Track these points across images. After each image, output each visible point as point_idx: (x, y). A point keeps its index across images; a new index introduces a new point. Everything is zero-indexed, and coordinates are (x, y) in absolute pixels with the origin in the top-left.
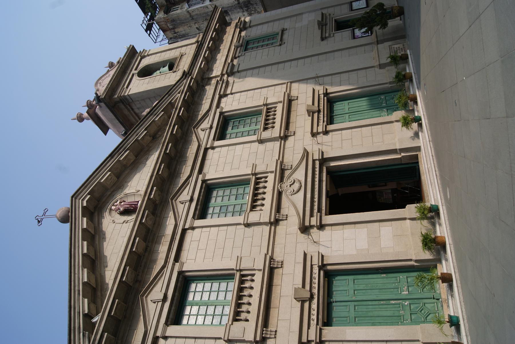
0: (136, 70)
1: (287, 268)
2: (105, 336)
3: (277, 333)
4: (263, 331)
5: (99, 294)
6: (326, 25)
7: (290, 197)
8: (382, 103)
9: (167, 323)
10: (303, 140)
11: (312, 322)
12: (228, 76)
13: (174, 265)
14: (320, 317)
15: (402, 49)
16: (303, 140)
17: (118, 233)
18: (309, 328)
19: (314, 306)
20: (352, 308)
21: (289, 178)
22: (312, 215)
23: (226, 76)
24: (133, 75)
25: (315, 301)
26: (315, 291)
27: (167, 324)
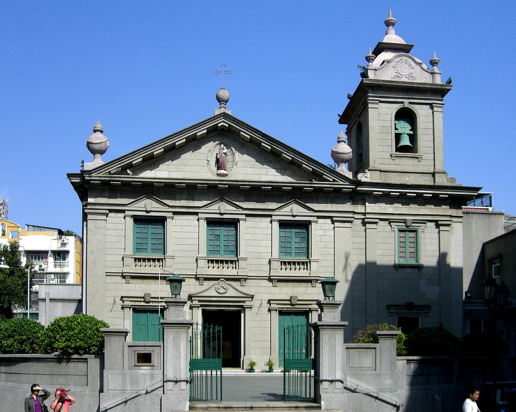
0: (410, 103)
7: (214, 287)
10: (263, 292)
12: (363, 219)
13: (171, 212)
18: (130, 301)
19: (143, 304)
20: (144, 323)
22: (199, 301)
23: (362, 217)
24: (403, 103)
26: (151, 304)
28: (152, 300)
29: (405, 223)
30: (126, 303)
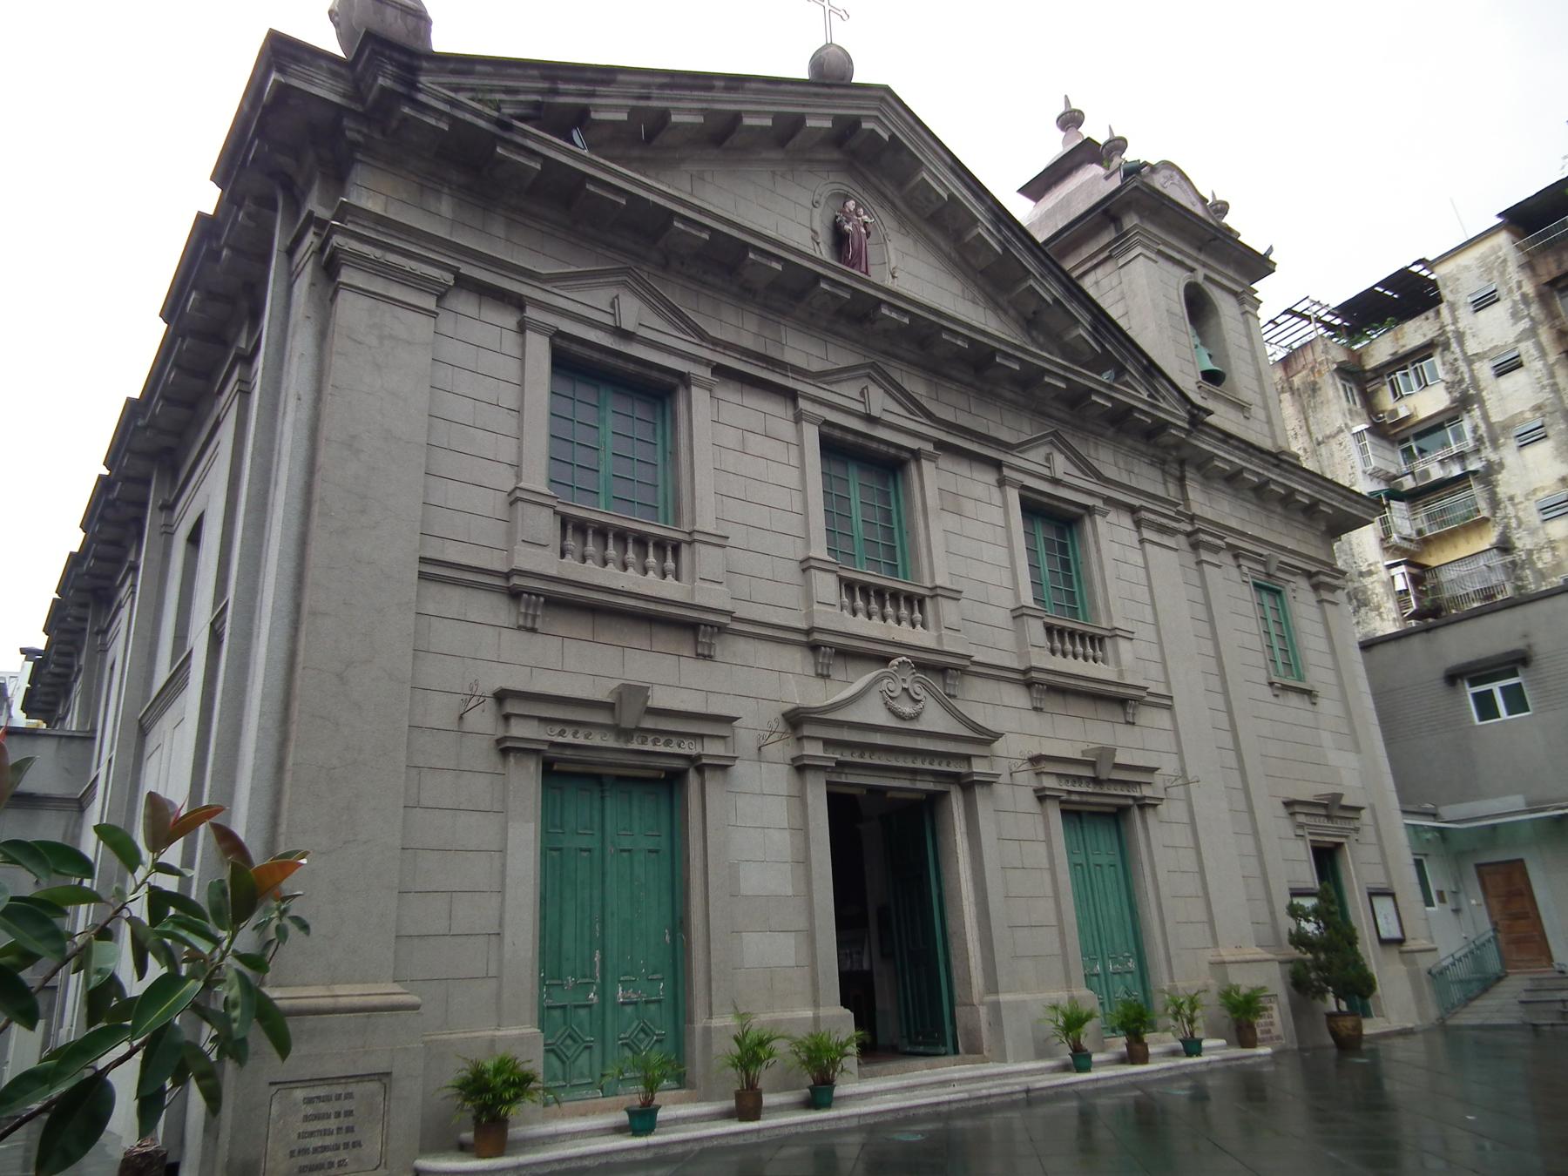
0: (1207, 278)
1: (694, 671)
2: (532, 164)
3: (527, 636)
4: (538, 595)
5: (635, 153)
6: (1328, 817)
7: (877, 689)
8: (1115, 960)
9: (559, 341)
10: (1022, 731)
11: (557, 729)
12: (1188, 535)
13: (708, 363)
14: (568, 753)
15: (1269, 1031)
16: (1022, 731)
17: (786, 214)
18: (541, 719)
19: (597, 740)
20: (584, 842)
21: (925, 687)
22: (828, 743)
23: (1189, 528)
24: (1192, 270)
25: (610, 742)
27: (557, 336)
28: (648, 723)
29: (1264, 564)
30: (519, 729)
